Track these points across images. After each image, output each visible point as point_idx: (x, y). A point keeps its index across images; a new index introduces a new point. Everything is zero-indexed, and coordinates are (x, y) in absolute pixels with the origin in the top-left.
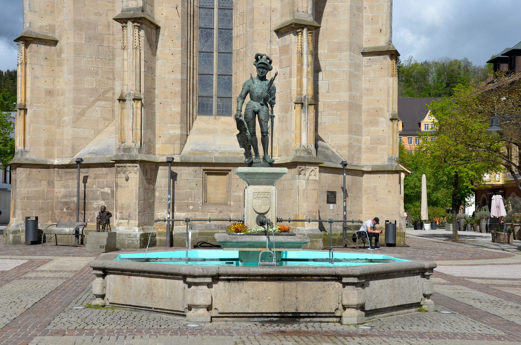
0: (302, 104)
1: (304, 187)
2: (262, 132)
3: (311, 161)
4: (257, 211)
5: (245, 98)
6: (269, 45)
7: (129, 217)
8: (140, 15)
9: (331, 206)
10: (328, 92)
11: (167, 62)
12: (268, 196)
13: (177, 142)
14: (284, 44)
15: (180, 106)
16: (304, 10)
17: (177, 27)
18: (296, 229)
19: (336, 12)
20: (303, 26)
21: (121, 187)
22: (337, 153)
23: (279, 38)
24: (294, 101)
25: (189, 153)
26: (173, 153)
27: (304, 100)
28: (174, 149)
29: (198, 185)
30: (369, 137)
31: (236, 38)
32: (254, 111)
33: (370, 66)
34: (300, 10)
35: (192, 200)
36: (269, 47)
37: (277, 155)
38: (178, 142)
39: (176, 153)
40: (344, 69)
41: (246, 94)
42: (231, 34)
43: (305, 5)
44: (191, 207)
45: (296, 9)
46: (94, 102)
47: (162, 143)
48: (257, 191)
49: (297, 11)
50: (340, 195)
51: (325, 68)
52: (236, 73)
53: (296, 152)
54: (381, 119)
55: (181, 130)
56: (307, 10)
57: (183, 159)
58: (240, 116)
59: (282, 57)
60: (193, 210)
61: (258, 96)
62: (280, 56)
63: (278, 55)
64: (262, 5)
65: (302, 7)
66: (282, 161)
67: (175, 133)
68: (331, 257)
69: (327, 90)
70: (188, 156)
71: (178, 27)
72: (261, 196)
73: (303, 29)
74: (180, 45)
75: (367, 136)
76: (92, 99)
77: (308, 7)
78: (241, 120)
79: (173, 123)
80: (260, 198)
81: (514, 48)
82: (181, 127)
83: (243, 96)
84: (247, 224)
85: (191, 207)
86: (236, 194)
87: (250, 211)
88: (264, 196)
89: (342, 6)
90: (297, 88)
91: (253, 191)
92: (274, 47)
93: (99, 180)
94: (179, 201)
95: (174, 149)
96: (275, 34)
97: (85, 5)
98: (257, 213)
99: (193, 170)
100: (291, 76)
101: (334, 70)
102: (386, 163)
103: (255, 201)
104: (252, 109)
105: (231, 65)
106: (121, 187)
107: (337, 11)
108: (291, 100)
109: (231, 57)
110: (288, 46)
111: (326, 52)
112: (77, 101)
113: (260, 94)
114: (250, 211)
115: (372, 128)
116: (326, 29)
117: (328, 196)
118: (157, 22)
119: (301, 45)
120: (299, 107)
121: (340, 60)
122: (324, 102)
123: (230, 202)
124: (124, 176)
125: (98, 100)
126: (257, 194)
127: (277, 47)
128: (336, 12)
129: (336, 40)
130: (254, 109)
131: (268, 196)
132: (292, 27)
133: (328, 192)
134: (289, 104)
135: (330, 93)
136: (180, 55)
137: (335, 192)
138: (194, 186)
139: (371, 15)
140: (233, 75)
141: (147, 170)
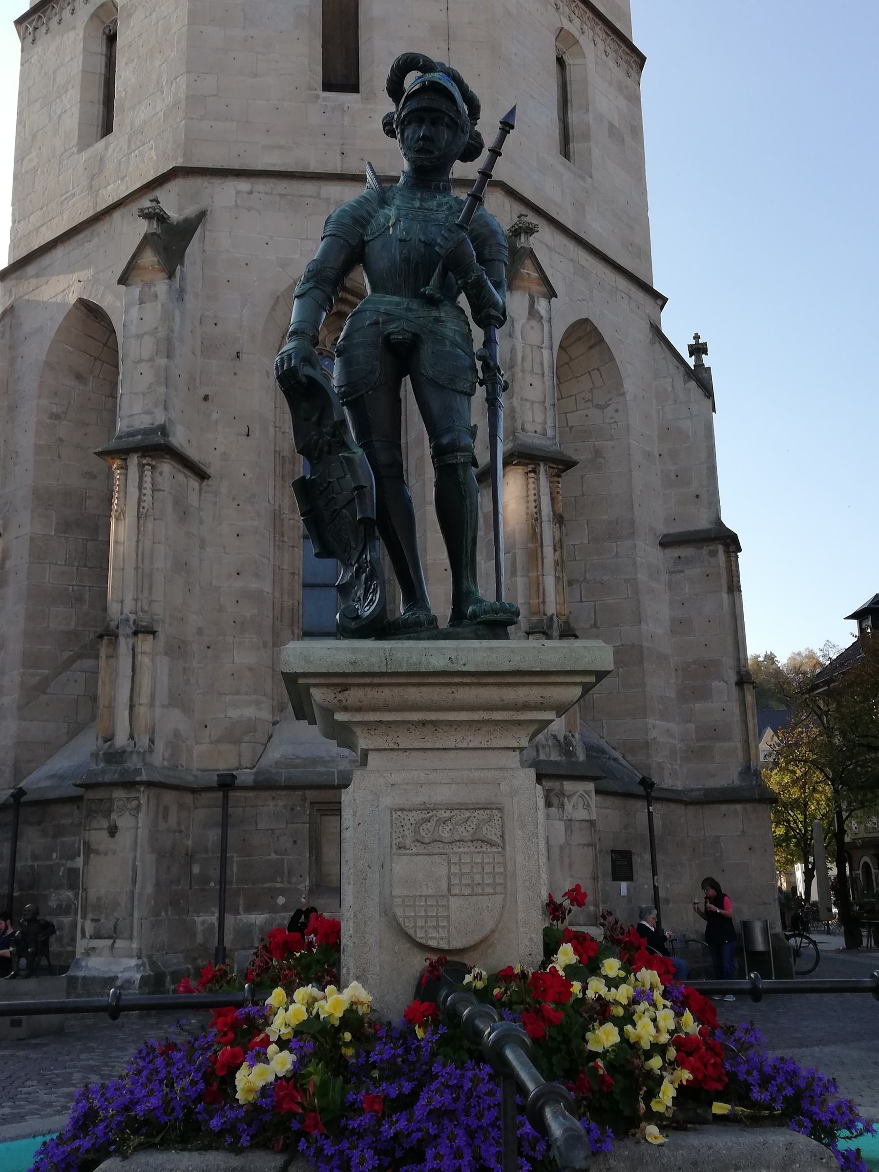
1: (562, 840)
4: (420, 936)
7: (115, 932)
8: (158, 439)
9: (624, 885)
10: (595, 625)
11: (225, 553)
12: (491, 832)
13: (246, 738)
16: (539, 428)
19: (602, 460)
21: (97, 853)
22: (624, 763)
25: (276, 763)
26: (237, 765)
27: (550, 627)
29: (299, 842)
30: (692, 726)
32: (387, 338)
33: (682, 571)
34: (529, 427)
35: (282, 882)
39: (245, 763)
40: (628, 577)
43: (539, 418)
46: (71, 661)
47: (211, 743)
48: (417, 800)
49: (523, 429)
50: (641, 861)
53: (538, 751)
54: (715, 684)
56: (545, 429)
61: (407, 260)
65: (534, 421)
71: (251, 475)
72: (445, 833)
75: (687, 722)
76: (66, 655)
77: (545, 423)
79: (238, 693)
80: (437, 848)
85: (281, 900)
88: (463, 832)
89: (613, 448)
91: (387, 801)
93: (64, 839)
94: (250, 885)
97: (59, 457)
99: (285, 807)
101: (605, 578)
102: (737, 783)
103: (401, 866)
106: (97, 853)
107: (604, 458)
111: (586, 542)
112: (30, 661)
115: (698, 706)
118: (202, 466)
121: (617, 556)
124: (105, 824)
125: (80, 656)
126: (415, 816)
128: (602, 460)
129: (606, 517)
130: (391, 328)
133: (612, 851)
135: (598, 628)
137: (630, 852)
141: (166, 809)
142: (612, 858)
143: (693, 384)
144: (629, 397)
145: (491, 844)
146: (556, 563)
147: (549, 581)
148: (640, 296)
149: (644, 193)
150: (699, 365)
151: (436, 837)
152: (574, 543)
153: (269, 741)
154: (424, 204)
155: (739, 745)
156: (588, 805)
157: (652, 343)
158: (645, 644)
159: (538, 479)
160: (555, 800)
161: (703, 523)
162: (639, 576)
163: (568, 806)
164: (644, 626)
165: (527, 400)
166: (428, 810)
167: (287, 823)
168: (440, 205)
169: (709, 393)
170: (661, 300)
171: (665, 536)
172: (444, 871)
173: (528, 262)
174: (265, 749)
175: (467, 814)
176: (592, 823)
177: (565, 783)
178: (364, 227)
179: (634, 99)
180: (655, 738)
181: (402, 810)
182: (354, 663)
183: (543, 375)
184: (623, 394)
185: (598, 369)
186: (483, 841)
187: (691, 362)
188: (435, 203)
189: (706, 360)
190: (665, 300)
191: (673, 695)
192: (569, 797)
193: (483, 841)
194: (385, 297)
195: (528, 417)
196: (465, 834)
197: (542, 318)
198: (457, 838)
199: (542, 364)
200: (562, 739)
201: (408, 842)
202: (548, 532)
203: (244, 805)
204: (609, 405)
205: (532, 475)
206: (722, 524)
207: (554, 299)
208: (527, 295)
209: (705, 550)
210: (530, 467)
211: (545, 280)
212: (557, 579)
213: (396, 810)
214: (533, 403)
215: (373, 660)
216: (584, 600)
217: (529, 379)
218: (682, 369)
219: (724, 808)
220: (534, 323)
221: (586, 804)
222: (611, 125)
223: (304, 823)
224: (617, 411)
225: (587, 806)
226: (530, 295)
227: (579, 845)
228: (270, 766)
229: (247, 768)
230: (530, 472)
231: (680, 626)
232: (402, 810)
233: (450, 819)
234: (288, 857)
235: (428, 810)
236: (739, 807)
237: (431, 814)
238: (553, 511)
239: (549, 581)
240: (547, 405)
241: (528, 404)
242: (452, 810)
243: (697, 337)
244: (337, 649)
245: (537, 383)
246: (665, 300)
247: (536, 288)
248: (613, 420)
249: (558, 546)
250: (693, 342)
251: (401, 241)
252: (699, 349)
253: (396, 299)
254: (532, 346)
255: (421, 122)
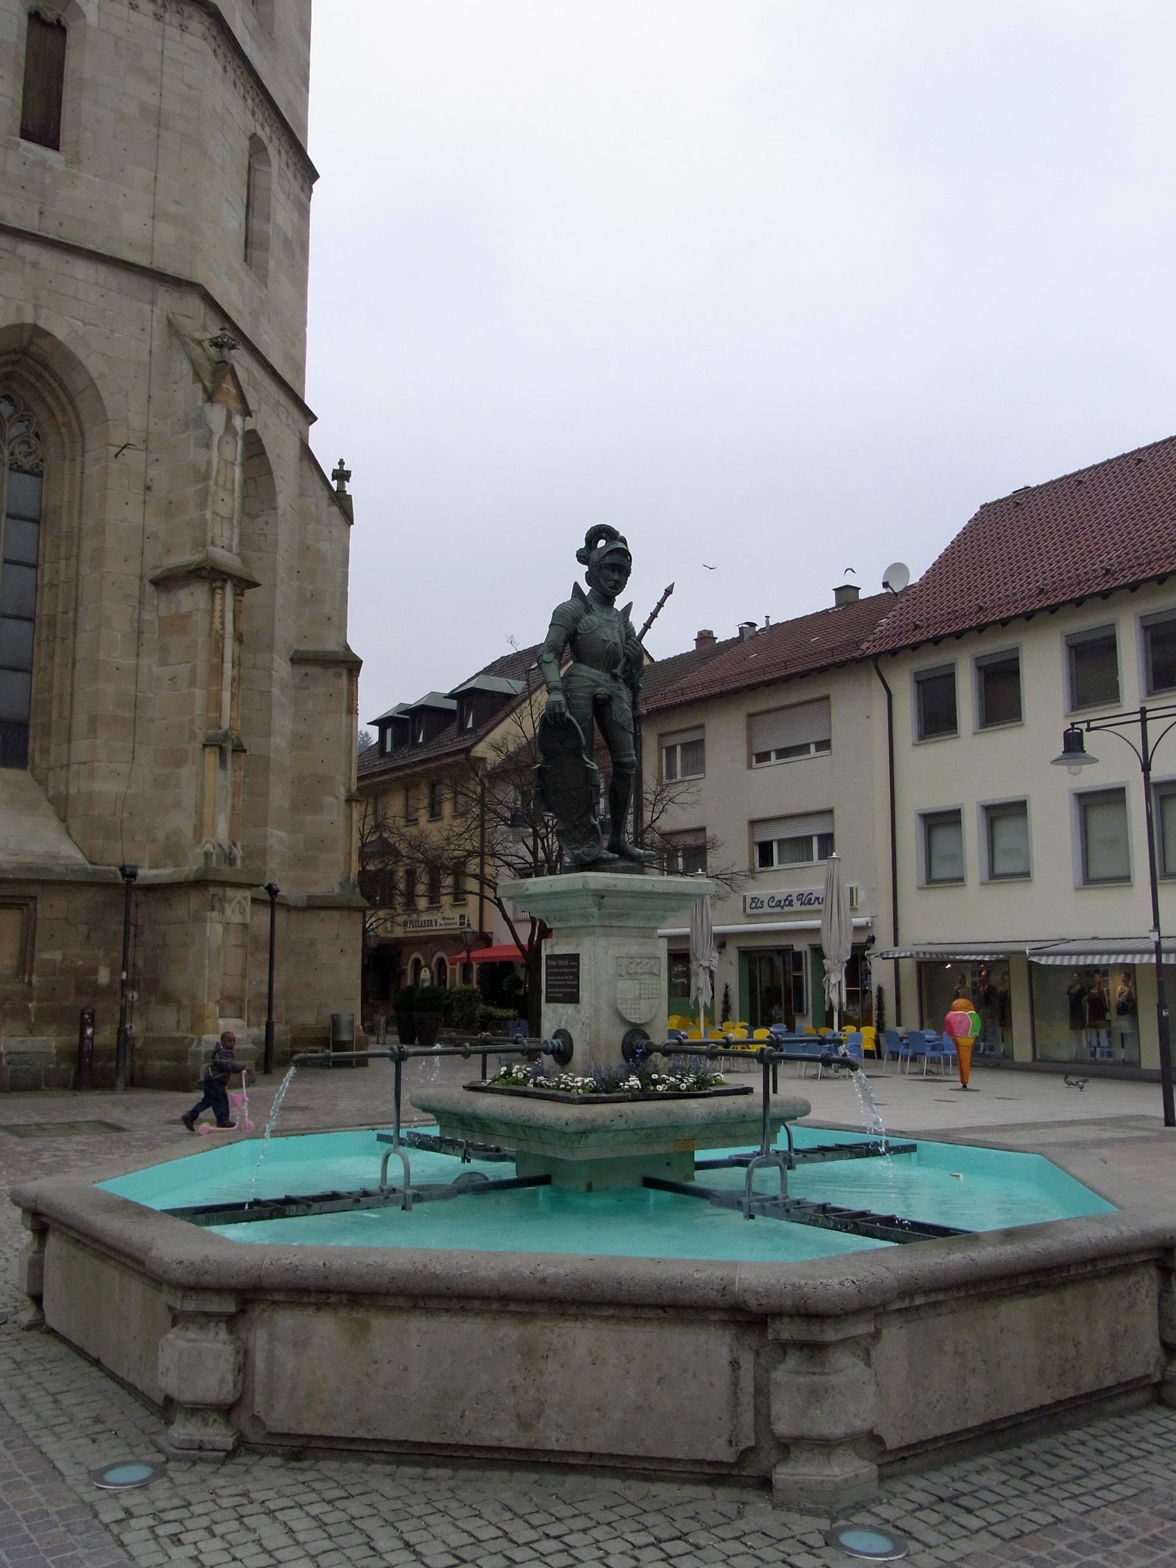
0: (222, 750)
4: (628, 1017)
6: (137, 612)
14: (173, 612)
16: (226, 542)
18: (200, 1040)
20: (225, 577)
32: (595, 696)
33: (306, 688)
37: (147, 865)
45: (210, 536)
54: (327, 799)
56: (231, 546)
63: (156, 636)
64: (124, 520)
73: (224, 581)
77: (231, 539)
81: (422, 703)
92: (147, 616)
96: (150, 588)
98: (625, 1022)
102: (337, 890)
103: (621, 984)
110: (188, 616)
119: (221, 617)
120: (212, 757)
123: (30, 976)
139: (310, 587)
143: (335, 509)
144: (280, 512)
145: (656, 975)
146: (233, 679)
147: (226, 696)
148: (296, 414)
149: (305, 309)
150: (341, 490)
155: (342, 858)
156: (244, 910)
157: (301, 460)
158: (272, 755)
159: (223, 595)
160: (217, 906)
161: (330, 646)
162: (273, 690)
163: (228, 912)
164: (272, 739)
165: (218, 515)
169: (349, 519)
170: (310, 418)
171: (296, 652)
172: (638, 987)
173: (229, 377)
176: (245, 926)
177: (227, 889)
179: (303, 211)
180: (271, 846)
182: (615, 885)
183: (233, 491)
184: (275, 508)
185: (254, 479)
187: (334, 484)
189: (349, 488)
190: (315, 419)
191: (287, 806)
192: (230, 902)
195: (218, 532)
197: (236, 434)
199: (233, 481)
200: (226, 847)
201: (624, 973)
202: (229, 646)
204: (260, 516)
205: (219, 591)
206: (348, 648)
207: (248, 418)
208: (225, 410)
209: (330, 672)
210: (219, 584)
211: (242, 398)
212: (233, 695)
214: (222, 517)
217: (223, 494)
218: (326, 492)
219: (322, 913)
220: (229, 438)
222: (286, 237)
224: (267, 523)
225: (243, 912)
226: (228, 409)
230: (219, 587)
231: (300, 741)
236: (336, 914)
238: (235, 629)
239: (226, 696)
240: (235, 522)
241: (219, 519)
243: (341, 463)
245: (227, 498)
246: (315, 419)
247: (235, 405)
248: (262, 532)
249: (237, 663)
250: (338, 467)
252: (342, 475)
253: (597, 671)
254: (226, 461)
255: (613, 570)
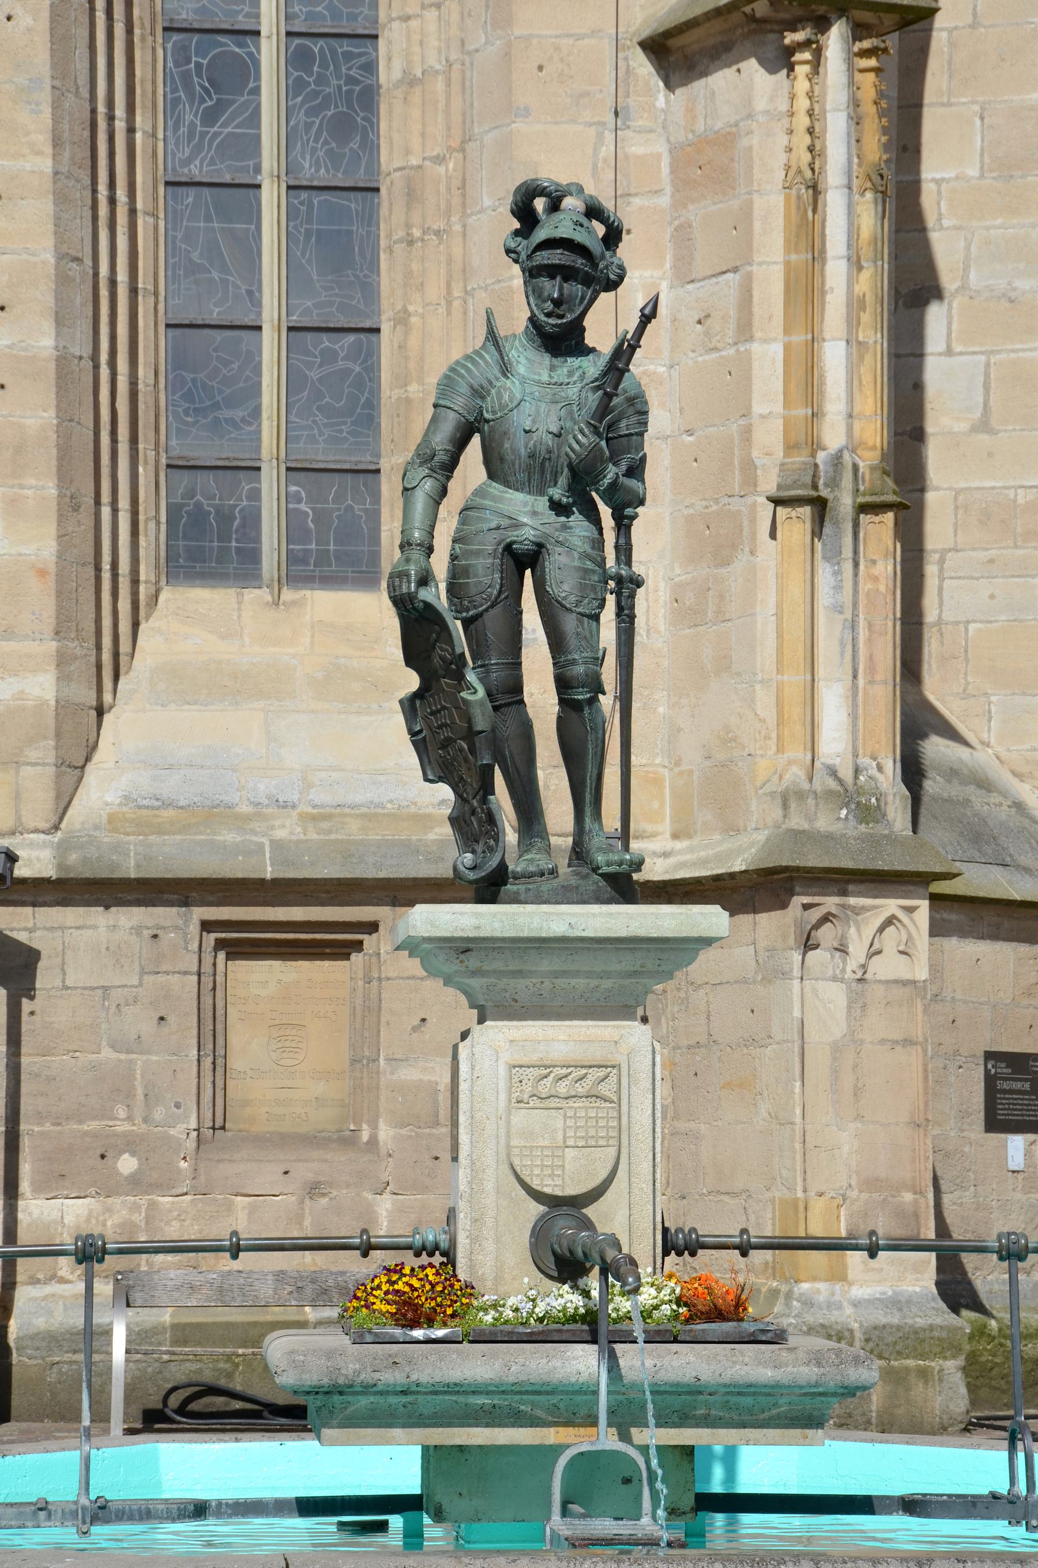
0: (820, 506)
1: (838, 1029)
2: (563, 684)
3: (880, 865)
4: (536, 1184)
5: (450, 466)
6: (609, 137)
10: (983, 426)
12: (607, 1089)
13: (33, 755)
14: (700, 126)
15: (51, 529)
17: (24, 20)
18: (789, 1295)
23: (669, 86)
24: (770, 484)
25: (111, 818)
26: (9, 824)
27: (834, 483)
28: (17, 797)
29: (172, 1019)
31: (399, 93)
32: (508, 548)
35: (130, 1118)
36: (607, 150)
37: (666, 826)
38: (44, 751)
41: (461, 443)
42: (371, 67)
44: (127, 1164)
48: (534, 1058)
51: (965, 277)
52: (402, 319)
53: (785, 806)
55: (63, 678)
57: (73, 858)
58: (425, 579)
59: (693, 213)
60: (136, 1183)
61: (532, 456)
62: (679, 204)
63: (664, 201)
66: (694, 864)
67: (21, 696)
68: (1022, 1488)
69: (978, 414)
70: (106, 838)
71: (29, 21)
72: (562, 1088)
74: (42, 139)
78: (428, 605)
80: (553, 1103)
82: (62, 660)
83: (441, 457)
84: (472, 1267)
85: (127, 1164)
86: (408, 1074)
87: (489, 1186)
90: (787, 405)
91: (506, 1057)
92: (636, 147)
94: (48, 1127)
95: (17, 797)
96: (643, 66)
98: (537, 1196)
99: (137, 930)
100: (745, 330)
103: (519, 1118)
104: (496, 535)
105: (374, 265)
108: (750, 479)
109: (371, 218)
111: (973, 172)
113: (549, 440)
114: (489, 1186)
116: (974, 26)
117: (990, 1081)
119: (811, 131)
122: (958, 492)
123: (374, 1126)
127: (660, 147)
130: (512, 536)
131: (605, 1089)
132: (752, 18)
133: (989, 1056)
134: (736, 504)
136: (46, 206)
138: (147, 1027)
140: (385, 328)
142: (987, 1072)
151: (553, 1093)
152: (938, 176)
153: (88, 759)
154: (552, 374)
166: (546, 1067)
167: (143, 972)
168: (571, 374)
172: (560, 1124)
174: (80, 779)
175: (584, 1071)
178: (483, 398)
181: (521, 1066)
182: (478, 928)
186: (597, 1097)
188: (565, 370)
193: (597, 1097)
194: (507, 492)
196: (580, 1090)
198: (573, 1093)
201: (526, 1097)
203: (30, 925)
213: (514, 1067)
215: (497, 925)
216: (958, 348)
221: (904, 937)
223: (186, 973)
227: (883, 1042)
228: (96, 827)
229: (36, 831)
232: (521, 1066)
233: (566, 1076)
234: (145, 1057)
235: (546, 1067)
237: (548, 1070)
242: (568, 1067)
244: (461, 914)
251: (526, 432)
